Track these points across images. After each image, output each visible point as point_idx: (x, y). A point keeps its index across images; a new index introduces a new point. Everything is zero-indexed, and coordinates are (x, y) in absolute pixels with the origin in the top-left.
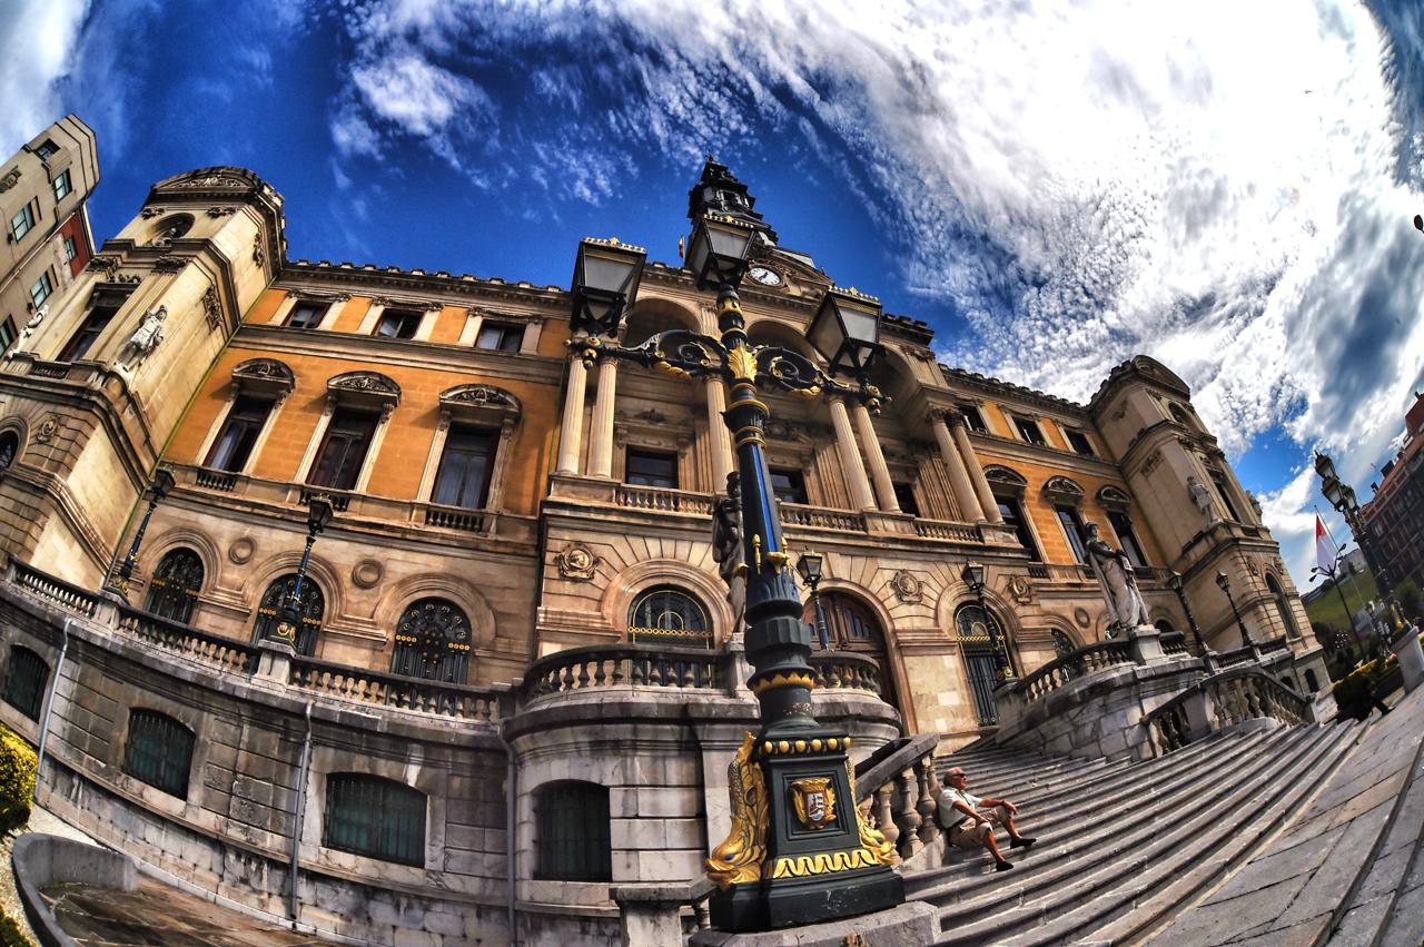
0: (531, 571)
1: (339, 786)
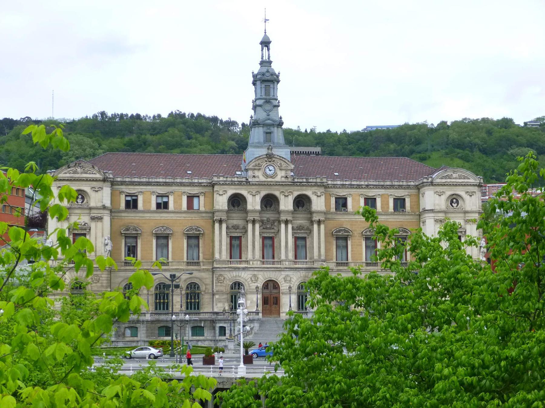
0: (211, 274)
1: (193, 328)
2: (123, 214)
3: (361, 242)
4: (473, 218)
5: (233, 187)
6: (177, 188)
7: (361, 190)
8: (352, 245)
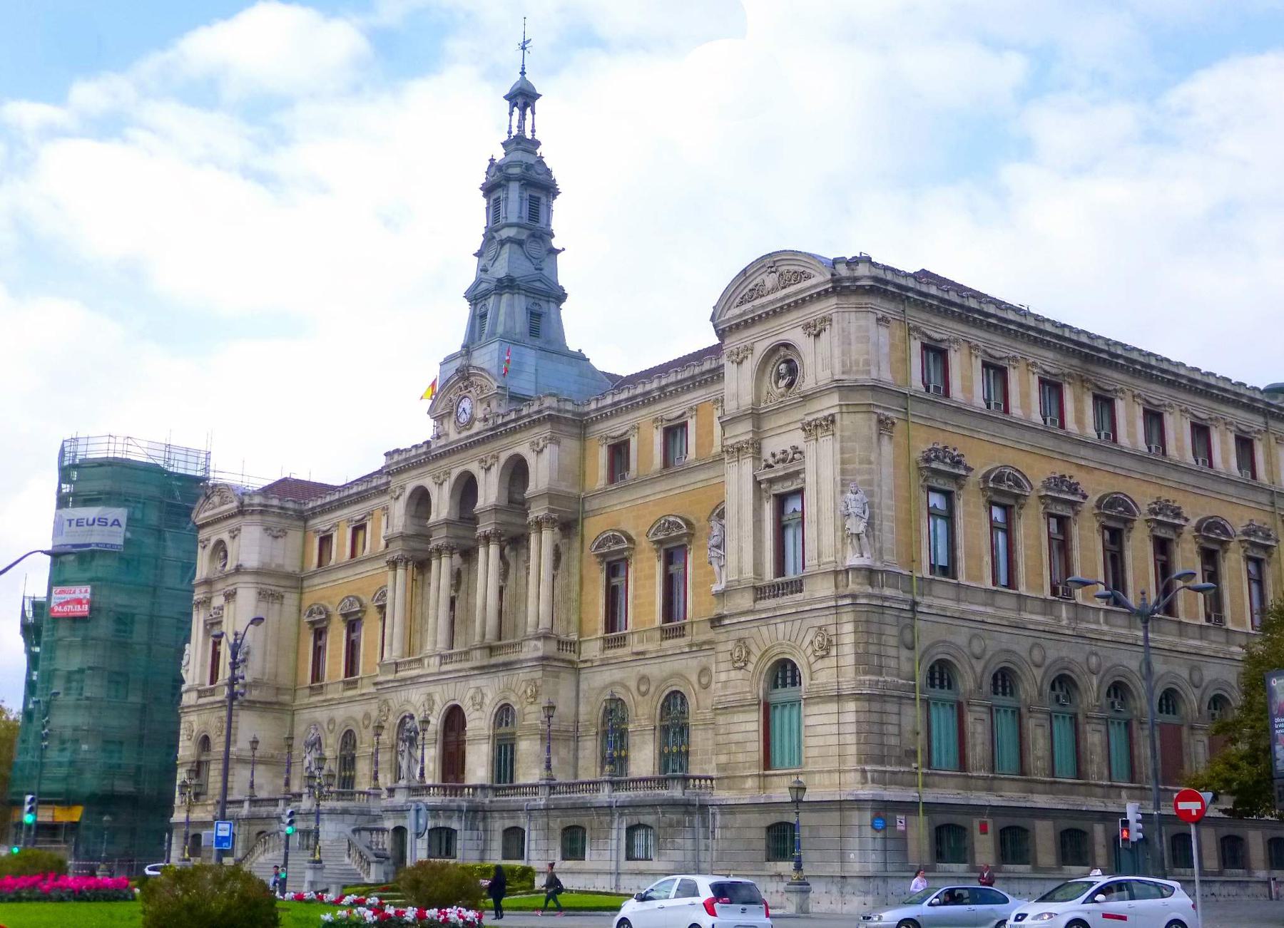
2: (316, 580)
3: (653, 567)
4: (826, 413)
5: (414, 473)
6: (377, 501)
7: (653, 408)
8: (635, 581)
